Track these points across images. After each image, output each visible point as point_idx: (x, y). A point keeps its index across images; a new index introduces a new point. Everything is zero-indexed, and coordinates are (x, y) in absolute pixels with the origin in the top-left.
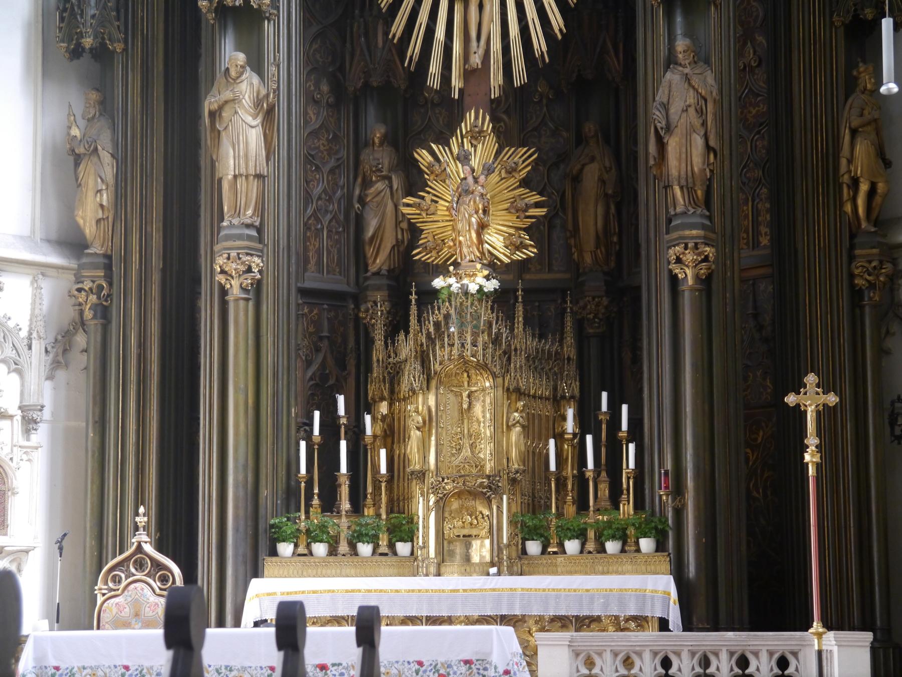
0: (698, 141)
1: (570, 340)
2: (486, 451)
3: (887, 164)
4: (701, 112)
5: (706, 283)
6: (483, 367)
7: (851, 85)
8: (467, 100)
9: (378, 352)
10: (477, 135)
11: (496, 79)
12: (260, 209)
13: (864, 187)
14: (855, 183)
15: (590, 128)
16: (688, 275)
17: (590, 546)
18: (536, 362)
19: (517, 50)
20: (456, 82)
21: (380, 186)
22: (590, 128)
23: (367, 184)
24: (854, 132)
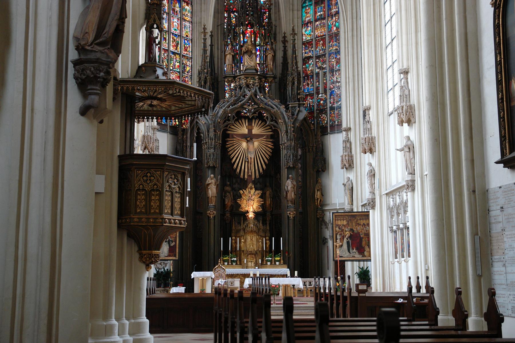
0: (293, 193)
1: (268, 226)
2: (255, 246)
3: (323, 195)
4: (294, 188)
5: (294, 217)
6: (255, 232)
7: (317, 181)
8: (248, 181)
9: (233, 228)
10: (251, 188)
11: (253, 177)
12: (215, 202)
13: (319, 200)
14: (318, 199)
15: (268, 184)
16: (291, 216)
17: (273, 263)
18: (265, 231)
19: (257, 172)
20: (246, 177)
21: (228, 194)
22: (268, 184)
23: (225, 193)
24: (318, 190)
